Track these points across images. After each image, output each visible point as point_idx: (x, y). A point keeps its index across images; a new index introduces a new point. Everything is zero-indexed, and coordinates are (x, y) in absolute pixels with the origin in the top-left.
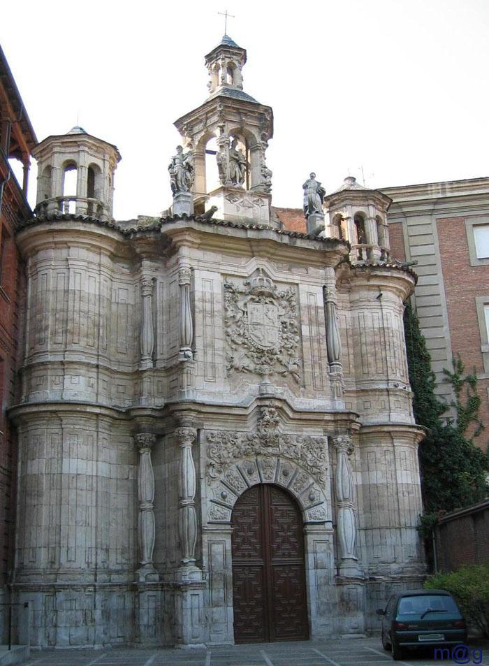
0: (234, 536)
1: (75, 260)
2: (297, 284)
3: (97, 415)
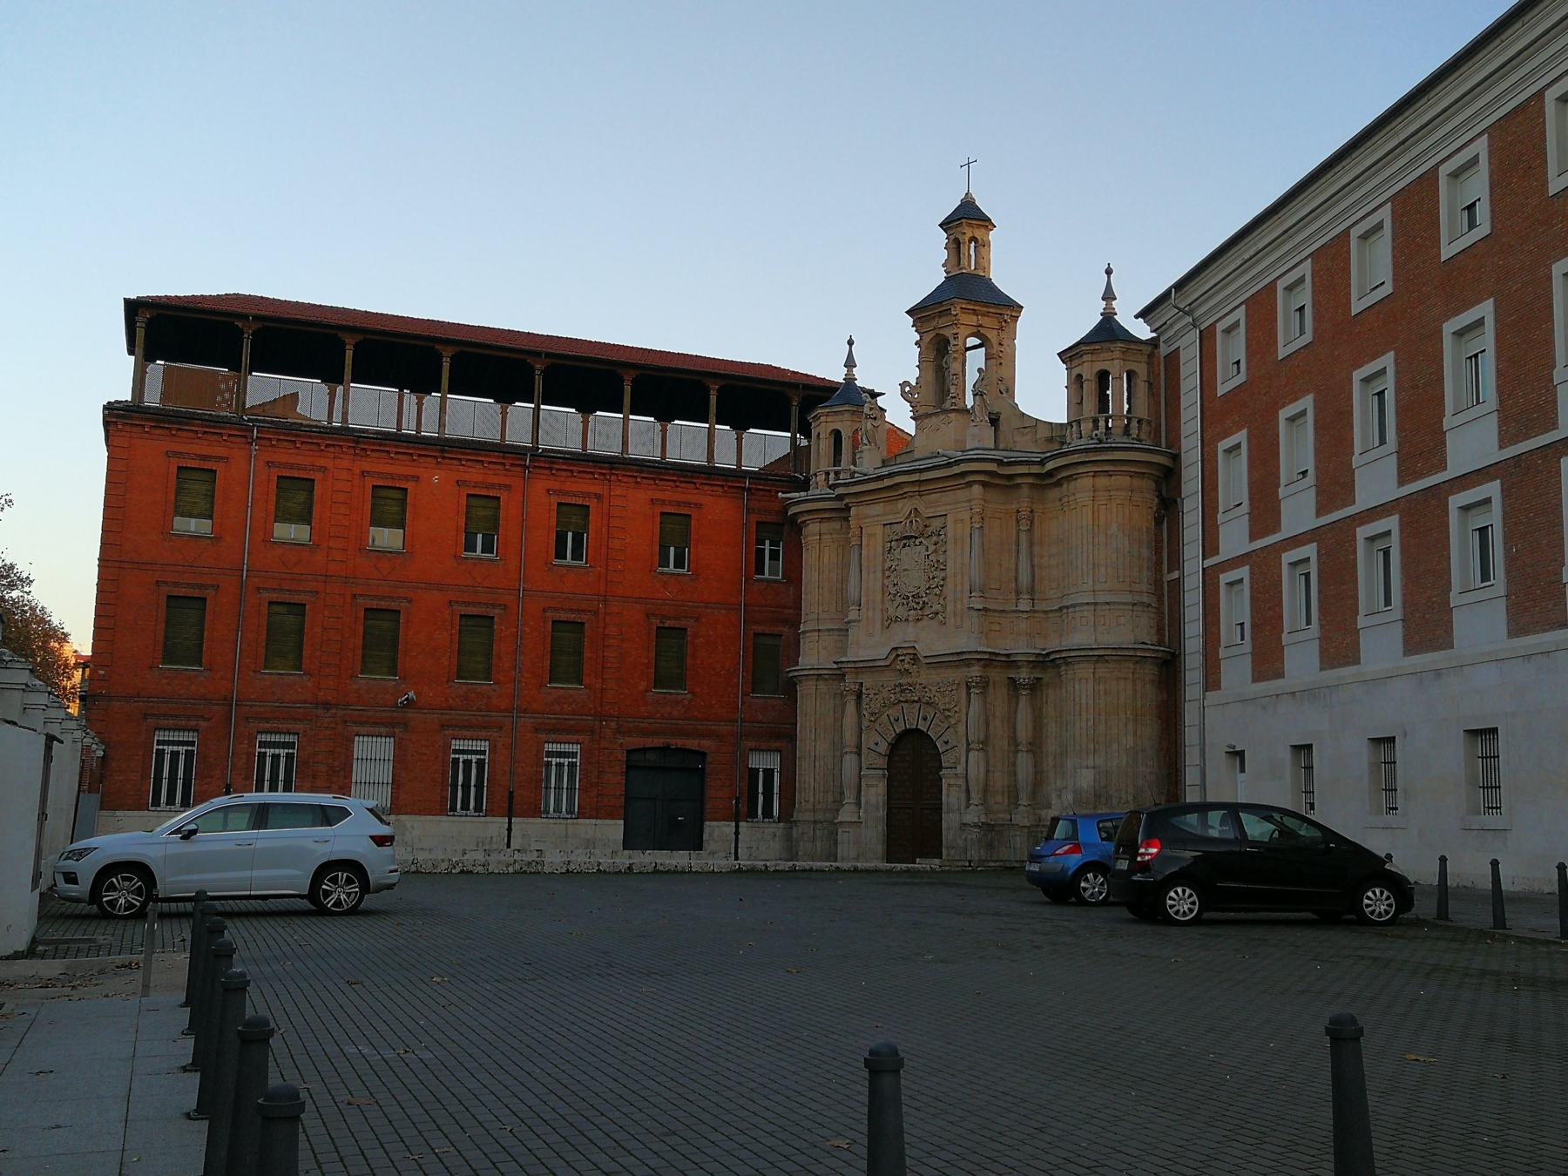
2: (946, 515)
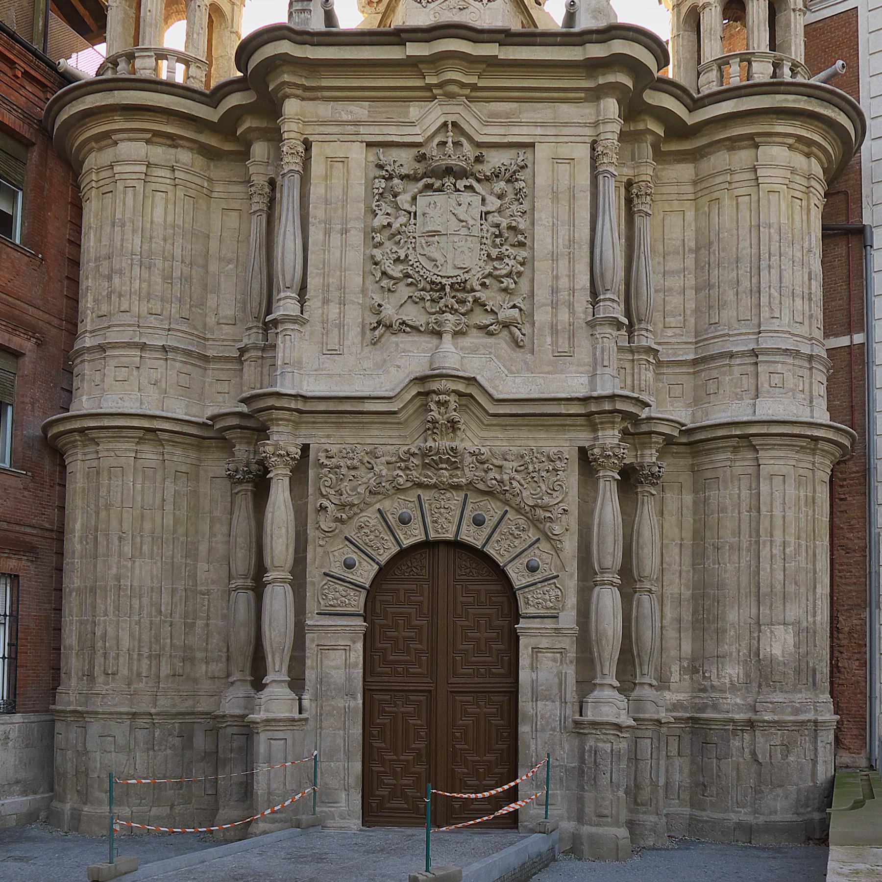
2: (532, 145)
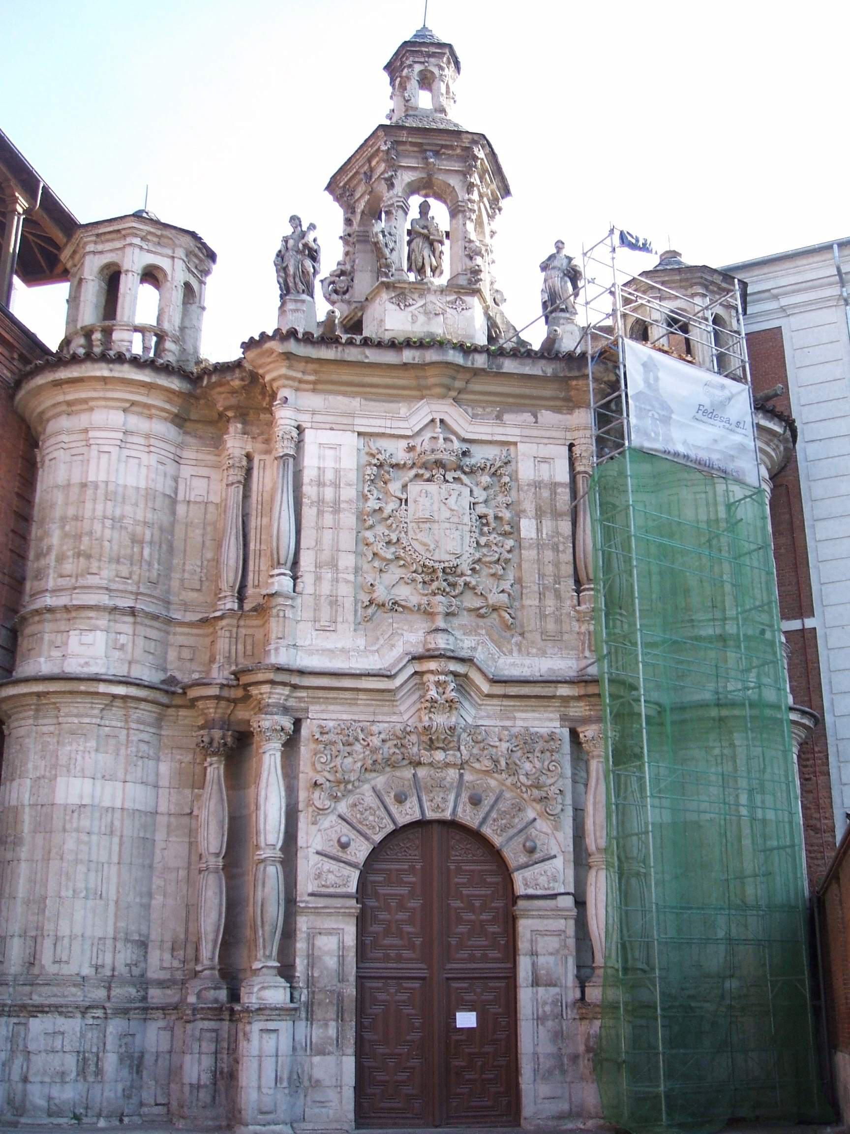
0: (362, 922)
1: (99, 429)
2: (515, 444)
3: (125, 698)
